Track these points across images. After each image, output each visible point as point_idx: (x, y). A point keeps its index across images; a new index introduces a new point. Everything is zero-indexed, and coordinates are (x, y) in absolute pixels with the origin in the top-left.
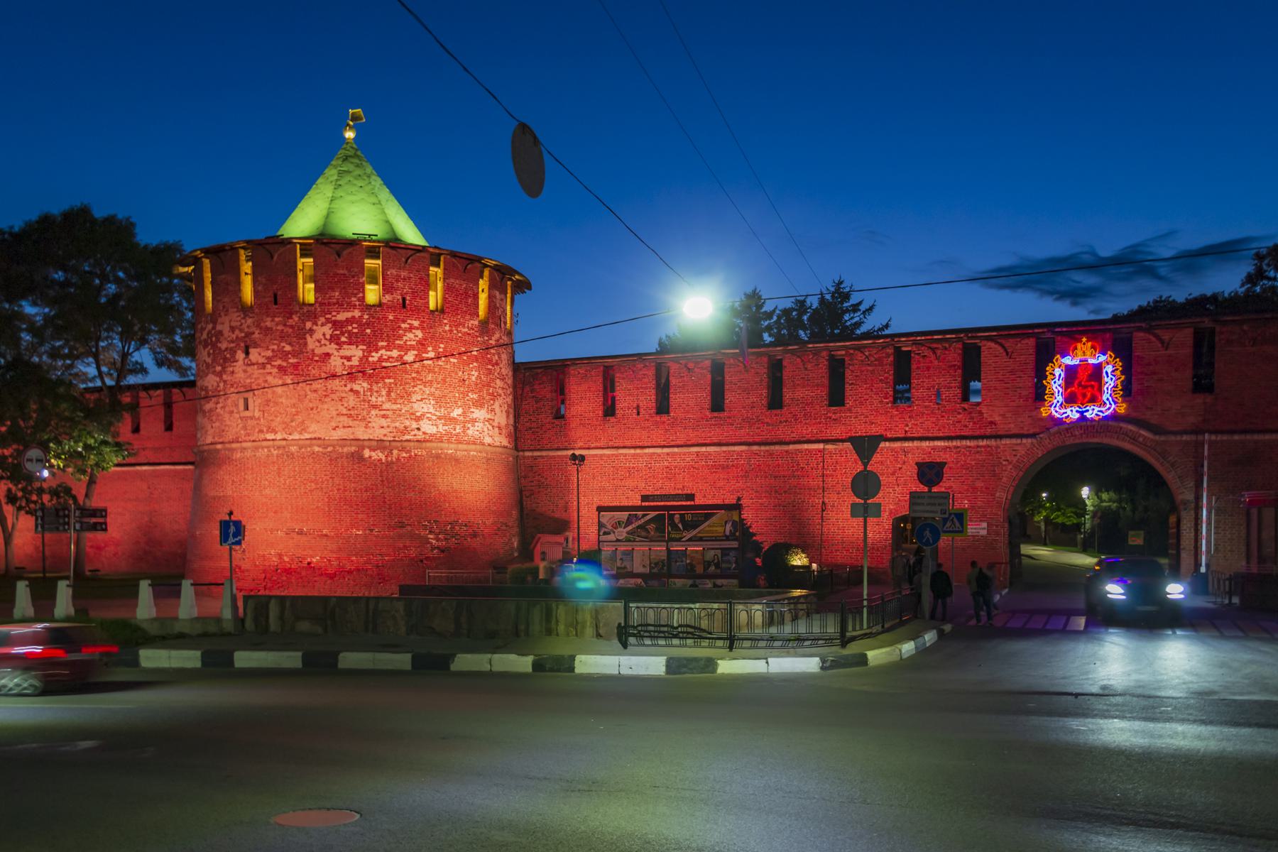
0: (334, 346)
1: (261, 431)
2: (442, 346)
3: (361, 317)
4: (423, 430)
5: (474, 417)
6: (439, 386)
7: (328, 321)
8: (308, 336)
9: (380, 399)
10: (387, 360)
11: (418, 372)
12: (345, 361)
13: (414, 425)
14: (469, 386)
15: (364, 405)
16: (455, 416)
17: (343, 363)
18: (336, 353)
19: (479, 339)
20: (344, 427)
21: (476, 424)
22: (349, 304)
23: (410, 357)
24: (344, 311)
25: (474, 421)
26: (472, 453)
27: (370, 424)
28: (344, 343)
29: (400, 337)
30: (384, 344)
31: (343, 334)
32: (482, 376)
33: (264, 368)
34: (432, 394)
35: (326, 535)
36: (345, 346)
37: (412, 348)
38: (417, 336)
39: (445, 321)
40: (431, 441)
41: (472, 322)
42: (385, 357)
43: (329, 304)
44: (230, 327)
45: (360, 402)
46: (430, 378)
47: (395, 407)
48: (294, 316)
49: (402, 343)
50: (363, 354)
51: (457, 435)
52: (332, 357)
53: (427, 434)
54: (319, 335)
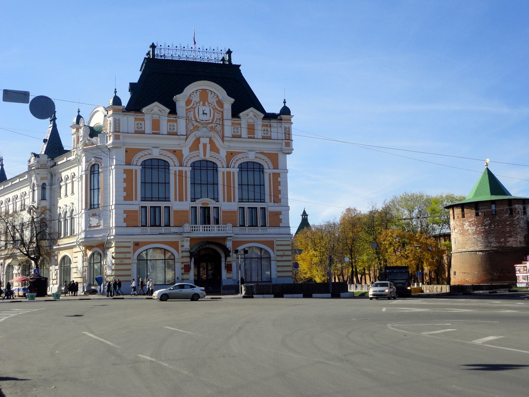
0: (469, 227)
1: (458, 249)
7: (468, 221)
10: (481, 229)
18: (470, 229)
21: (510, 242)
22: (472, 217)
25: (509, 242)
29: (484, 223)
31: (471, 224)
33: (457, 234)
39: (497, 217)
49: (485, 224)
54: (466, 225)
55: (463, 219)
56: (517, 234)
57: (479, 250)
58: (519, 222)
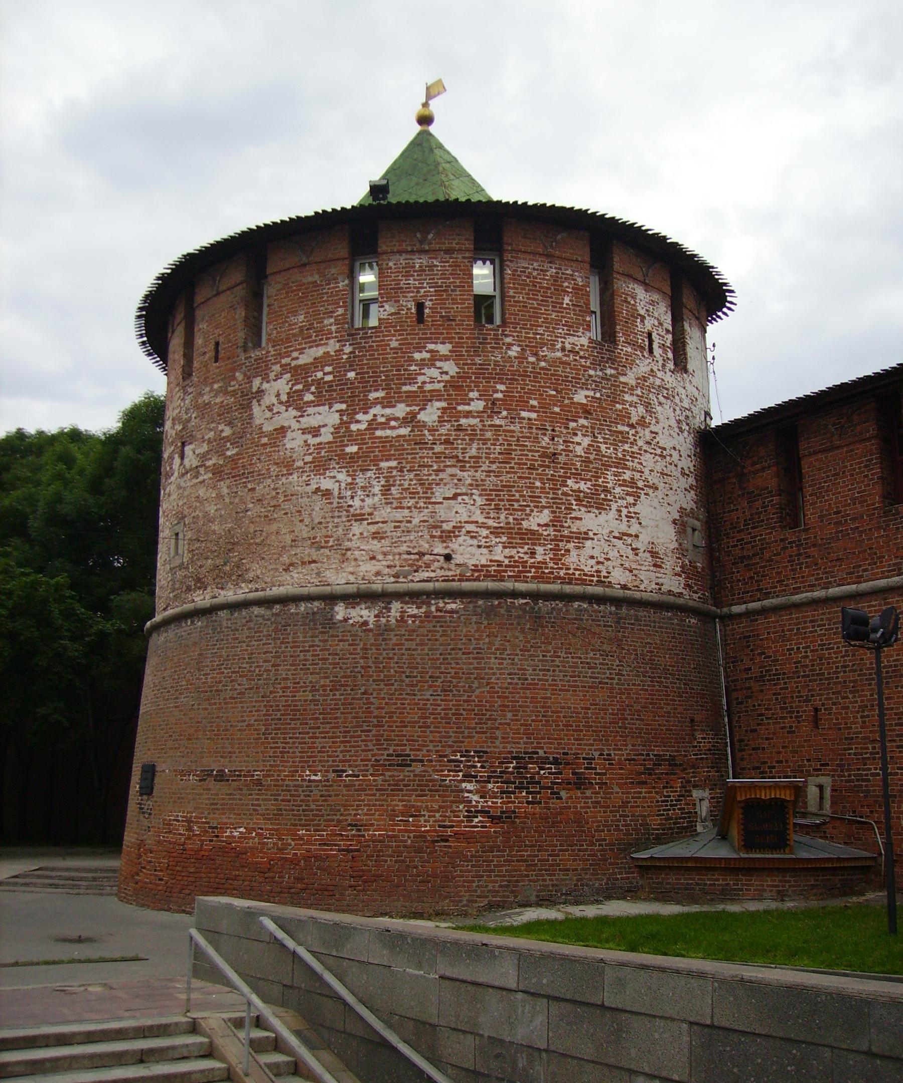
0: (293, 412)
2: (501, 387)
3: (339, 351)
5: (583, 530)
6: (494, 467)
7: (286, 368)
8: (255, 402)
9: (369, 501)
10: (385, 425)
11: (447, 442)
12: (309, 437)
15: (339, 517)
16: (536, 528)
17: (306, 441)
18: (294, 425)
19: (592, 372)
20: (303, 563)
21: (588, 543)
23: (430, 415)
24: (310, 347)
28: (309, 404)
30: (380, 394)
31: (307, 388)
32: (603, 447)
34: (476, 484)
36: (311, 410)
37: (435, 395)
38: (447, 373)
39: (509, 340)
40: (477, 579)
42: (383, 420)
43: (288, 340)
45: (332, 512)
46: (473, 452)
47: (399, 515)
49: (414, 388)
50: (341, 419)
51: (538, 566)
52: (289, 435)
54: (269, 399)
56: (634, 490)
57: (352, 589)
58: (648, 405)
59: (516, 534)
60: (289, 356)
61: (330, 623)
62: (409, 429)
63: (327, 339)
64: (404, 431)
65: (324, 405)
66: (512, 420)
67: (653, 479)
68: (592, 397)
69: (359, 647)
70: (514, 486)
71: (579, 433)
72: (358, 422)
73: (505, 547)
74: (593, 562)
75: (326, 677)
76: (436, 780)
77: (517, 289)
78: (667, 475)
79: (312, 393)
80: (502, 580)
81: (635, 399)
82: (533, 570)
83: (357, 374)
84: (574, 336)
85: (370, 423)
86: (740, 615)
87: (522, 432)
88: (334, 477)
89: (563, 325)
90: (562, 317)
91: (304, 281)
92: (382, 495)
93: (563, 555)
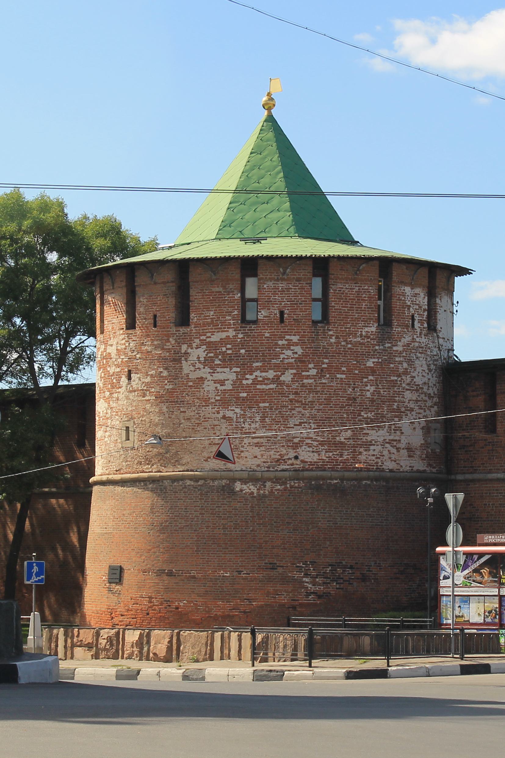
2: (326, 361)
4: (301, 458)
6: (321, 407)
7: (203, 343)
9: (253, 426)
11: (296, 393)
12: (218, 385)
13: (292, 454)
14: (361, 405)
16: (343, 440)
17: (216, 388)
18: (210, 378)
19: (377, 348)
21: (372, 448)
23: (287, 377)
24: (218, 332)
25: (368, 445)
26: (364, 482)
27: (242, 454)
29: (277, 356)
31: (216, 356)
34: (313, 417)
35: (194, 577)
36: (219, 370)
37: (290, 366)
38: (296, 353)
39: (331, 333)
40: (312, 470)
41: (366, 329)
42: (261, 379)
43: (204, 325)
44: (117, 350)
46: (310, 399)
48: (171, 339)
50: (237, 377)
52: (206, 382)
53: (307, 462)
54: (193, 358)
55: (182, 330)
57: (245, 475)
59: (333, 444)
60: (205, 335)
61: (232, 492)
62: (275, 385)
63: (228, 328)
64: (272, 386)
65: (227, 367)
66: (332, 379)
67: (412, 405)
68: (377, 362)
69: (249, 506)
70: (332, 418)
71: (369, 384)
72: (247, 379)
73: (326, 452)
74: (374, 458)
75: (231, 522)
76: (290, 576)
77: (336, 301)
78: (419, 401)
79: (220, 360)
80: (324, 470)
81: (402, 359)
82: (341, 464)
83: (246, 351)
84: (368, 326)
85: (254, 380)
86: (461, 481)
87: (337, 386)
88: (234, 410)
89: (362, 321)
90: (361, 316)
91: (214, 290)
92: (261, 422)
93: (358, 455)
